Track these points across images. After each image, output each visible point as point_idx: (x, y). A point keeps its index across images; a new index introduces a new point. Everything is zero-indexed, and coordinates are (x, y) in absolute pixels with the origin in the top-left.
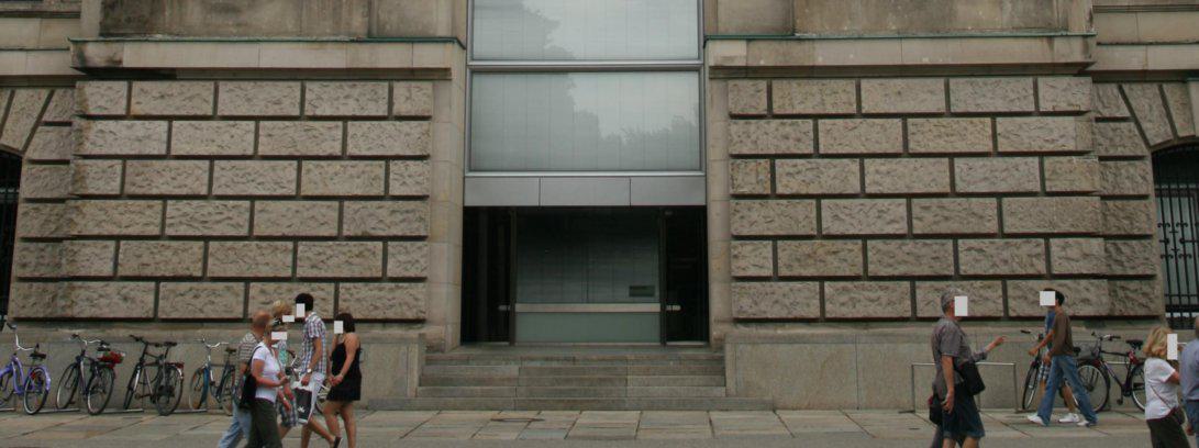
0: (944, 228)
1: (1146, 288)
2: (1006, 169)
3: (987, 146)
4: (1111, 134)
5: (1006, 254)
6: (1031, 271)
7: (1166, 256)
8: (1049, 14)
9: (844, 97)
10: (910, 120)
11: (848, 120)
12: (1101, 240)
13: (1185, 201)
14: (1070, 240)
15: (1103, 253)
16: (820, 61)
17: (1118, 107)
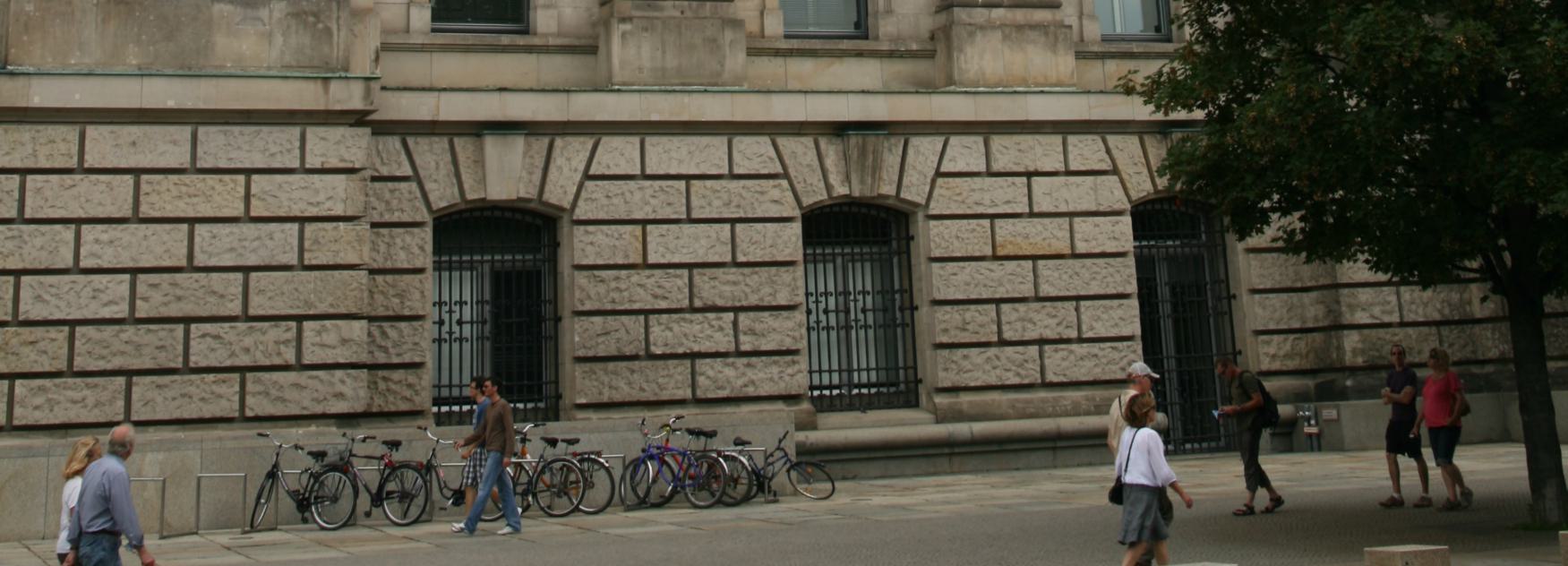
0: (174, 310)
1: (411, 379)
2: (259, 238)
3: (237, 209)
4: (387, 196)
5: (248, 341)
6: (277, 361)
7: (439, 341)
8: (326, 49)
9: (63, 147)
10: (144, 177)
11: (65, 177)
12: (364, 323)
13: (467, 274)
14: (327, 323)
15: (365, 338)
16: (37, 101)
17: (400, 164)
